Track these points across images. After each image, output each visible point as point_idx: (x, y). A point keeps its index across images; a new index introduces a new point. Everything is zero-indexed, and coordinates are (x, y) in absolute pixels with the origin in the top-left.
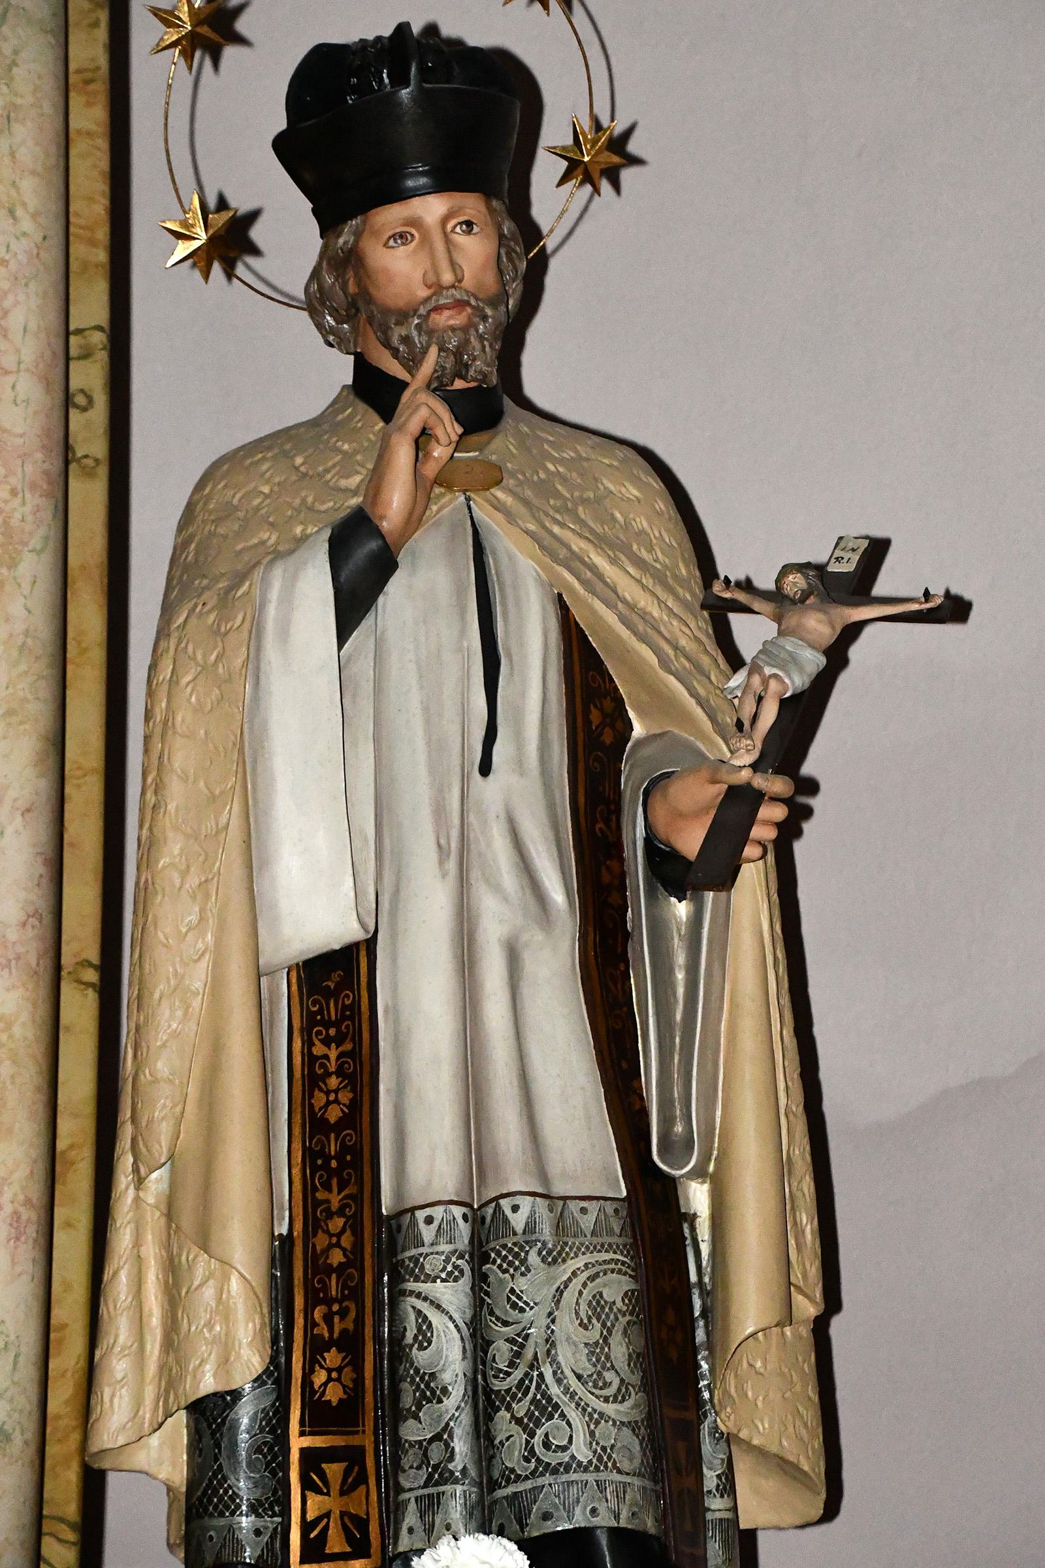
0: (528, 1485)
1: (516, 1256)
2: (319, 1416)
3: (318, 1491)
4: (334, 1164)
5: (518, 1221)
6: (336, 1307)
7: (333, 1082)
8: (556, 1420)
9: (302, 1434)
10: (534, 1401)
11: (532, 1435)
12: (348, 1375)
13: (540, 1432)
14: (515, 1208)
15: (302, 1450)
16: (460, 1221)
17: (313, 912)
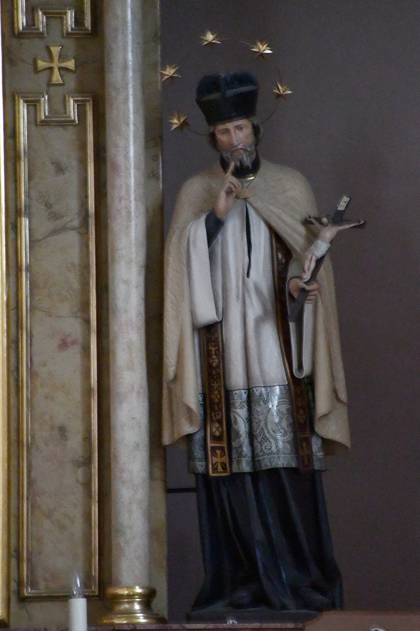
0: (262, 458)
1: (257, 402)
2: (215, 438)
3: (215, 456)
4: (215, 377)
5: (257, 393)
6: (217, 413)
7: (214, 357)
8: (268, 442)
9: (211, 443)
10: (263, 438)
11: (262, 446)
12: (220, 429)
13: (264, 446)
14: (257, 390)
15: (212, 447)
16: (244, 394)
17: (207, 313)
